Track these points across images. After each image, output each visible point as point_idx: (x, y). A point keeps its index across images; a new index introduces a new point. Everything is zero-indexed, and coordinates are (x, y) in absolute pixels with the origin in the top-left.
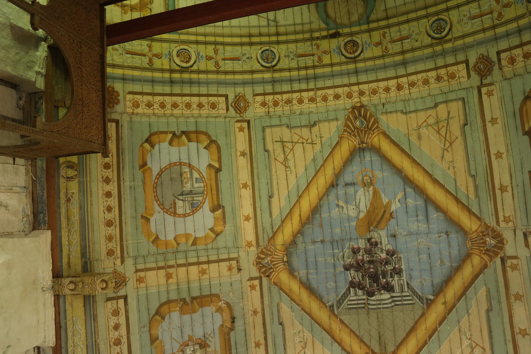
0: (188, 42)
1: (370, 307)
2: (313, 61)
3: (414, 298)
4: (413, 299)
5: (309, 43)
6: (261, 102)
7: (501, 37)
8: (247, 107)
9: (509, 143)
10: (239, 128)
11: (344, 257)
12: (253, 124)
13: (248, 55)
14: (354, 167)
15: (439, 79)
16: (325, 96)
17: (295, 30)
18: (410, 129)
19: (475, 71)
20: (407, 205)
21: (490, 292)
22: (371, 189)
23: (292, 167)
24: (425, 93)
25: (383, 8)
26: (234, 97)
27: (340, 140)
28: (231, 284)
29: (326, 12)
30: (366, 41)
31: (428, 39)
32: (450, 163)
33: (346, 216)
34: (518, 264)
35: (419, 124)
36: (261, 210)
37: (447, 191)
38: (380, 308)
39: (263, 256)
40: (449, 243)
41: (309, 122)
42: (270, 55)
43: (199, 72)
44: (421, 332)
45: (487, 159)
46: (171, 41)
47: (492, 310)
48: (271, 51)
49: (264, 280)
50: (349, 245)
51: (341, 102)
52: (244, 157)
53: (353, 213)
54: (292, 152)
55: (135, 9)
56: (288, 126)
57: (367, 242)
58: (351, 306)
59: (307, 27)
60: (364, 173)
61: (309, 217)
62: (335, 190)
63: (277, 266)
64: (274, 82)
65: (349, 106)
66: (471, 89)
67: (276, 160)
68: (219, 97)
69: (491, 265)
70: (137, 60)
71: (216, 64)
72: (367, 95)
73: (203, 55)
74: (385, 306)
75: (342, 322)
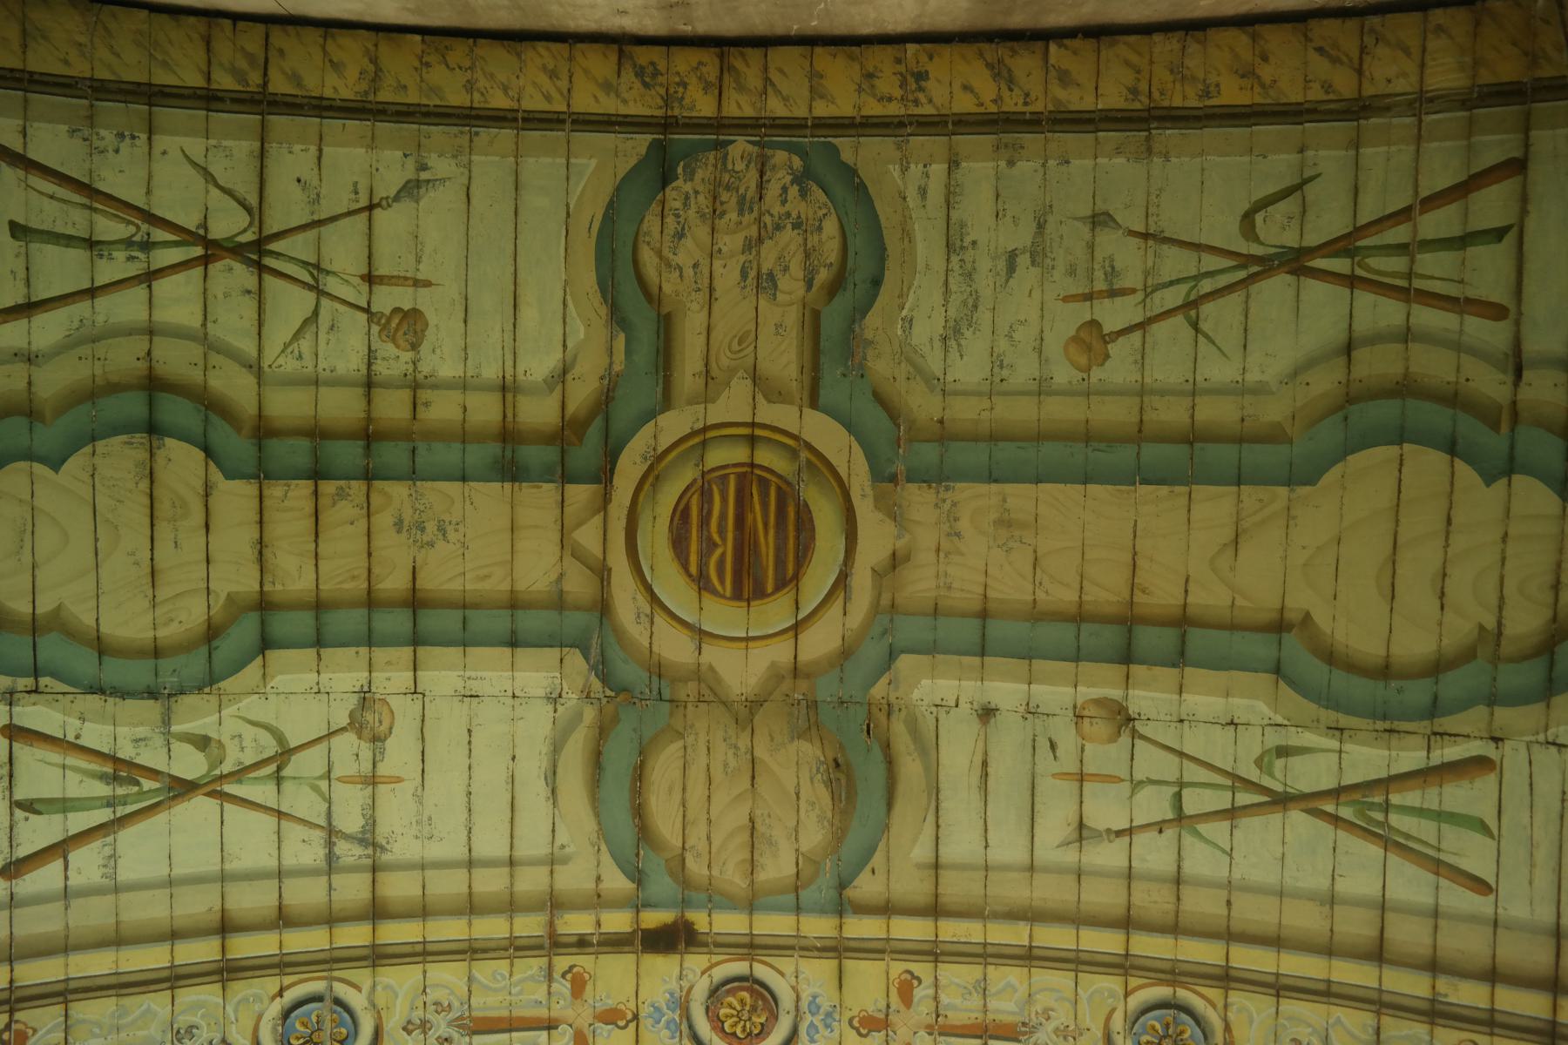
5: (532, 966)
17: (470, 894)
25: (921, 852)
29: (639, 812)
30: (815, 997)
42: (327, 1025)
48: (338, 1002)
59: (531, 882)
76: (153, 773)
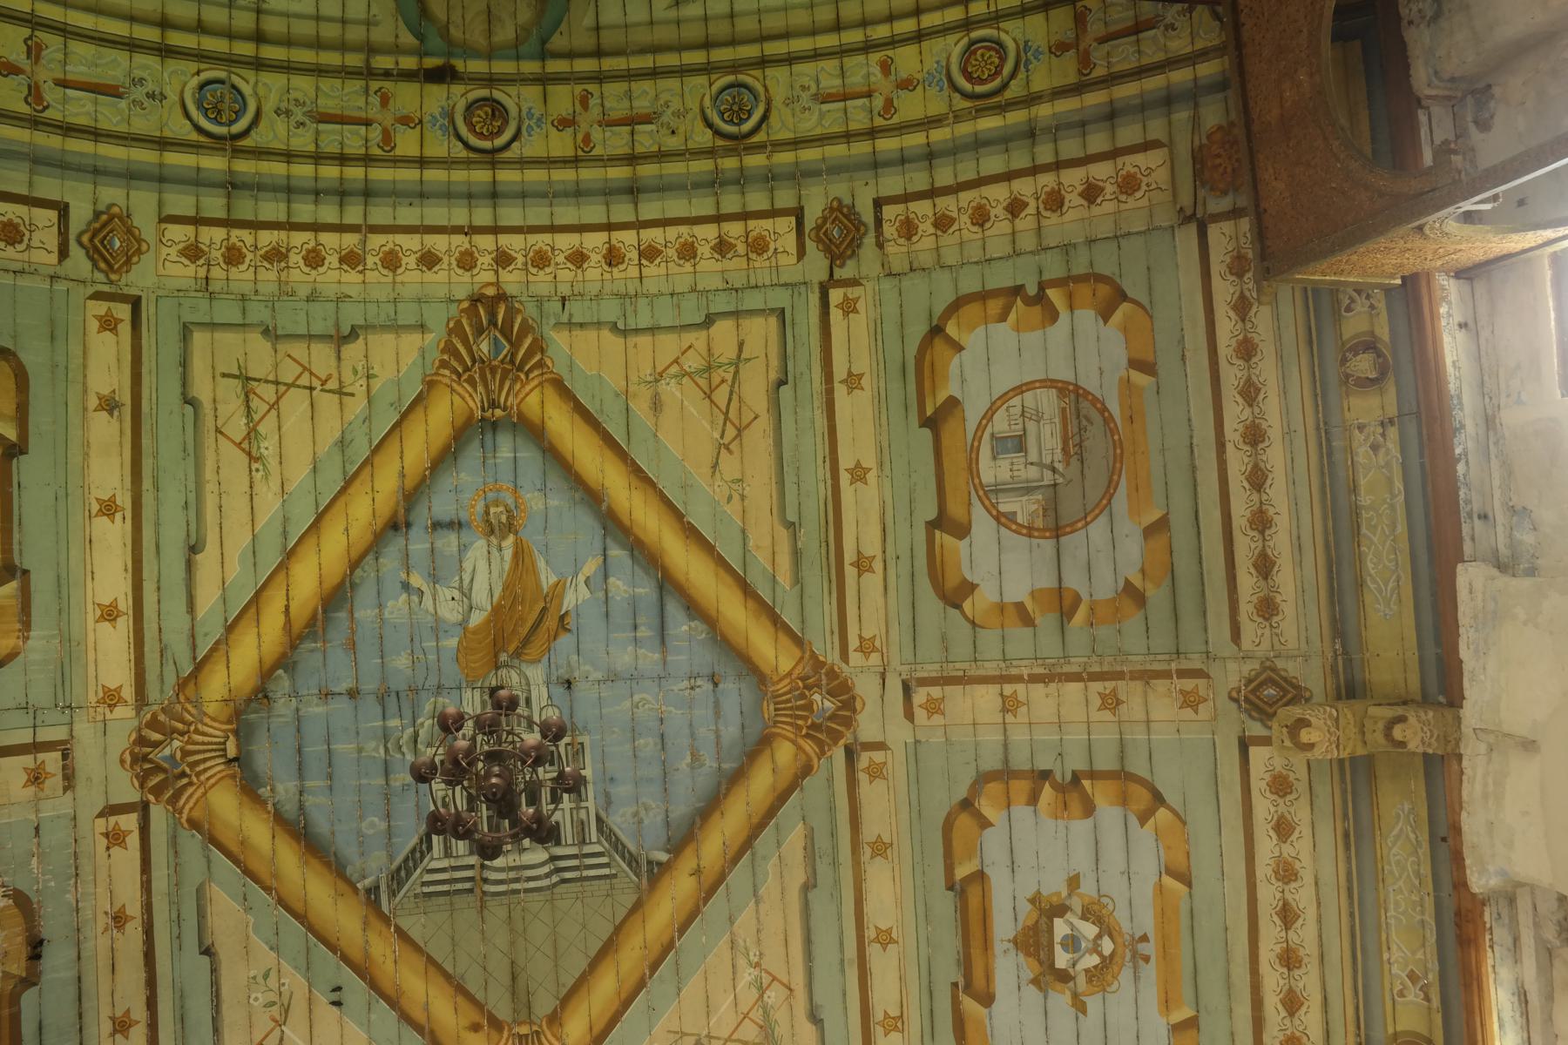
1: (487, 888)
2: (367, 141)
3: (615, 860)
4: (613, 864)
5: (357, 85)
6: (181, 246)
7: (888, 164)
8: (133, 255)
9: (885, 444)
10: (99, 318)
11: (416, 741)
12: (152, 310)
13: (150, 86)
14: (462, 475)
15: (722, 247)
16: (391, 252)
17: (318, 36)
18: (634, 378)
19: (819, 240)
20: (610, 595)
21: (813, 839)
22: (509, 542)
23: (270, 460)
24: (683, 284)
25: (589, 21)
26: (89, 215)
27: (428, 391)
28: (37, 829)
30: (530, 109)
31: (704, 134)
32: (733, 486)
33: (430, 618)
34: (885, 763)
35: (659, 370)
36: (159, 589)
37: (721, 562)
38: (517, 892)
39: (156, 736)
40: (717, 704)
41: (337, 325)
44: (631, 956)
45: (829, 482)
47: (815, 886)
48: (234, 87)
49: (158, 813)
50: (432, 707)
51: (438, 276)
52: (111, 414)
53: (450, 612)
54: (273, 413)
56: (266, 332)
57: (486, 697)
58: (432, 889)
59: (356, 34)
60: (490, 495)
61: (314, 617)
62: (401, 541)
63: (202, 767)
64: (234, 186)
65: (461, 293)
66: (803, 289)
67: (221, 433)
69: (820, 765)
72: (519, 266)
74: (532, 884)
75: (402, 934)
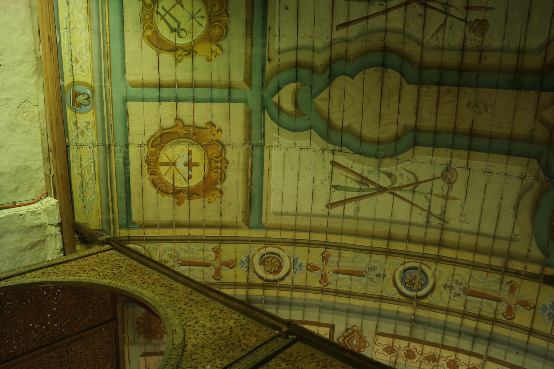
0: (279, 242)
2: (496, 310)
5: (496, 277)
6: (385, 346)
8: (361, 348)
13: (378, 271)
17: (476, 245)
26: (344, 330)
42: (418, 278)
43: (293, 288)
46: (251, 241)
48: (422, 271)
55: (195, 194)
59: (501, 246)
64: (415, 322)
68: (319, 326)
70: (196, 273)
71: (322, 278)
73: (302, 263)
76: (373, 183)
